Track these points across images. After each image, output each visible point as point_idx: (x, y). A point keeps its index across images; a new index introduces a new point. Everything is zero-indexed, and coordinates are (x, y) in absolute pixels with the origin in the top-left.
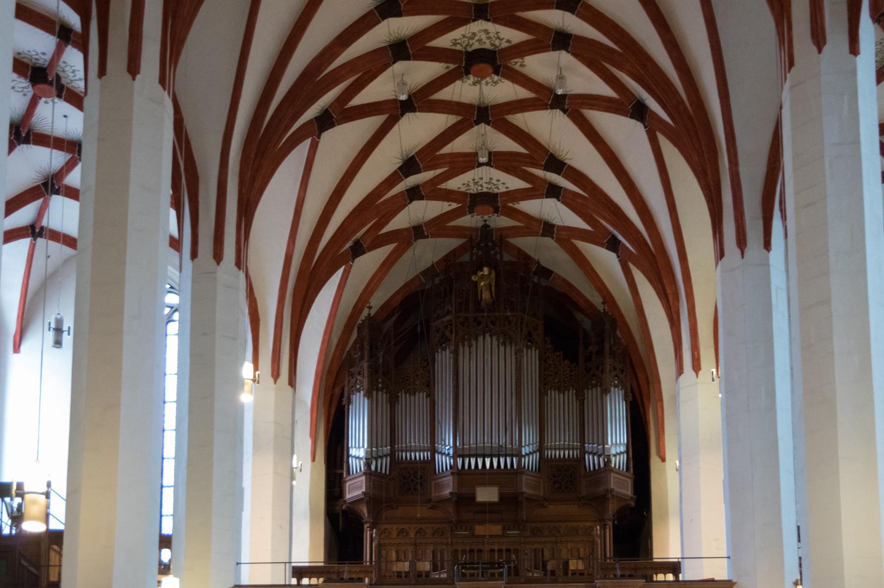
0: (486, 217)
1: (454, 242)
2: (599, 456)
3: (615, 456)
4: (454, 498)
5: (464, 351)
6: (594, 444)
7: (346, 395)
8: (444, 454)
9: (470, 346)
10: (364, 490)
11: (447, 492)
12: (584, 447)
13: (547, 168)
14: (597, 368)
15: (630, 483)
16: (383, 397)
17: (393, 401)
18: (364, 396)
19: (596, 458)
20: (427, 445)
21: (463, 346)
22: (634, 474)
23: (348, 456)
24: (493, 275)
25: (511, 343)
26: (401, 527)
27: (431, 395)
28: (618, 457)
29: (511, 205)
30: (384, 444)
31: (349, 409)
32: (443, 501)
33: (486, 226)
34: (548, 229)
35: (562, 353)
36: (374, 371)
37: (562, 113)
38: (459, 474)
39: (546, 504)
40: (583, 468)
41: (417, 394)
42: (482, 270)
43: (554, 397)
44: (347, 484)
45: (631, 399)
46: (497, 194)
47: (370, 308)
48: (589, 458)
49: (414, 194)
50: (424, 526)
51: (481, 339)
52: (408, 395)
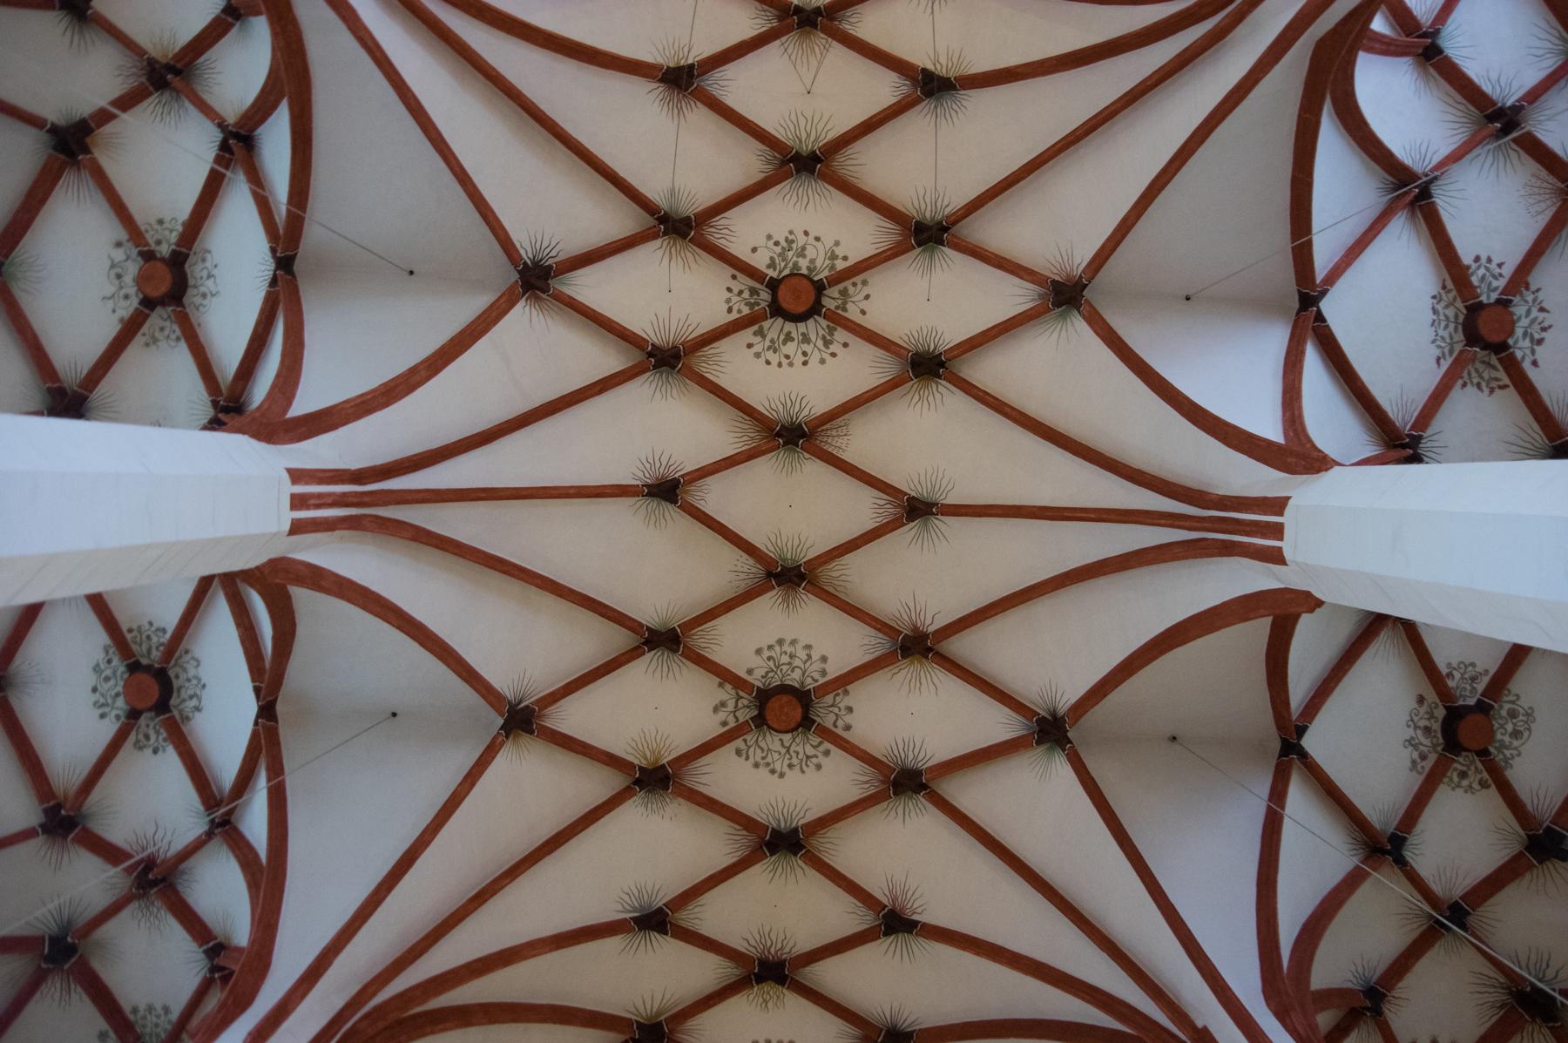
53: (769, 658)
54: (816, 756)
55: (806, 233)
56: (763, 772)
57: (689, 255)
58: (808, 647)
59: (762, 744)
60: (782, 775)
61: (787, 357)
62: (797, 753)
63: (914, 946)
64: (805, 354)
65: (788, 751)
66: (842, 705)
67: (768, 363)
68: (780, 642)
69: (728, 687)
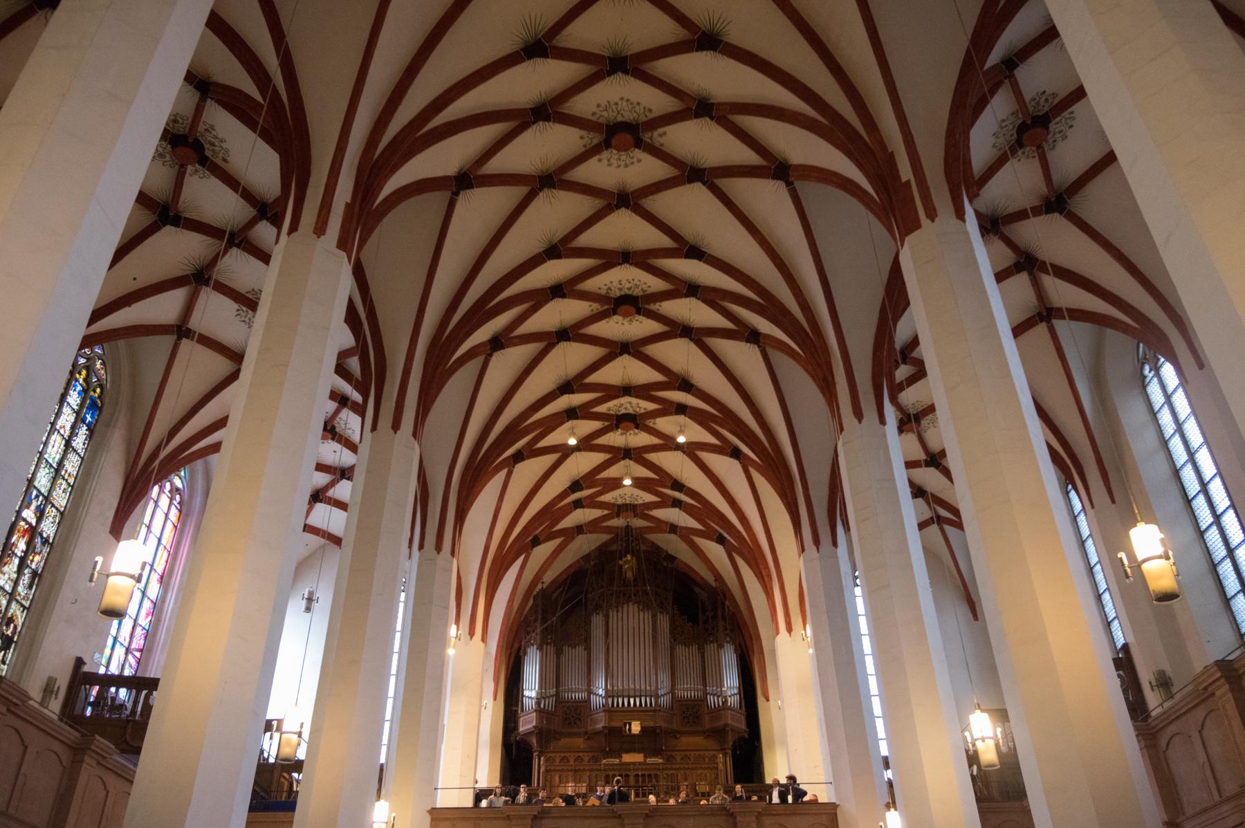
0: (628, 520)
1: (605, 537)
2: (719, 696)
3: (730, 696)
4: (606, 731)
5: (613, 615)
6: (713, 687)
7: (523, 648)
8: (598, 695)
9: (617, 612)
10: (534, 724)
11: (600, 726)
12: (706, 690)
13: (673, 488)
14: (713, 628)
15: (743, 718)
16: (551, 650)
17: (559, 653)
18: (537, 649)
19: (716, 698)
20: (585, 687)
21: (613, 611)
22: (746, 711)
23: (523, 696)
24: (634, 558)
25: (648, 610)
26: (562, 755)
27: (588, 649)
28: (733, 697)
29: (646, 512)
30: (551, 687)
31: (524, 659)
32: (597, 733)
33: (627, 526)
34: (673, 528)
35: (686, 616)
36: (545, 631)
37: (682, 454)
38: (610, 711)
39: (678, 736)
40: (706, 707)
41: (577, 647)
42: (625, 556)
43: (681, 650)
44: (521, 719)
45: (740, 652)
46: (637, 505)
47: (543, 583)
48: (710, 699)
49: (578, 504)
50: (581, 754)
51: (625, 606)
52: (570, 648)
53: (633, 157)
54: (601, 111)
55: (623, 324)
56: (634, 99)
57: (679, 317)
58: (609, 165)
59: (635, 115)
60: (622, 99)
61: (630, 282)
62: (613, 111)
63: (524, 34)
64: (621, 284)
65: (618, 112)
66: (587, 139)
67: (640, 281)
68: (626, 166)
69: (657, 145)
